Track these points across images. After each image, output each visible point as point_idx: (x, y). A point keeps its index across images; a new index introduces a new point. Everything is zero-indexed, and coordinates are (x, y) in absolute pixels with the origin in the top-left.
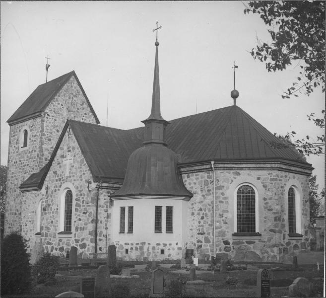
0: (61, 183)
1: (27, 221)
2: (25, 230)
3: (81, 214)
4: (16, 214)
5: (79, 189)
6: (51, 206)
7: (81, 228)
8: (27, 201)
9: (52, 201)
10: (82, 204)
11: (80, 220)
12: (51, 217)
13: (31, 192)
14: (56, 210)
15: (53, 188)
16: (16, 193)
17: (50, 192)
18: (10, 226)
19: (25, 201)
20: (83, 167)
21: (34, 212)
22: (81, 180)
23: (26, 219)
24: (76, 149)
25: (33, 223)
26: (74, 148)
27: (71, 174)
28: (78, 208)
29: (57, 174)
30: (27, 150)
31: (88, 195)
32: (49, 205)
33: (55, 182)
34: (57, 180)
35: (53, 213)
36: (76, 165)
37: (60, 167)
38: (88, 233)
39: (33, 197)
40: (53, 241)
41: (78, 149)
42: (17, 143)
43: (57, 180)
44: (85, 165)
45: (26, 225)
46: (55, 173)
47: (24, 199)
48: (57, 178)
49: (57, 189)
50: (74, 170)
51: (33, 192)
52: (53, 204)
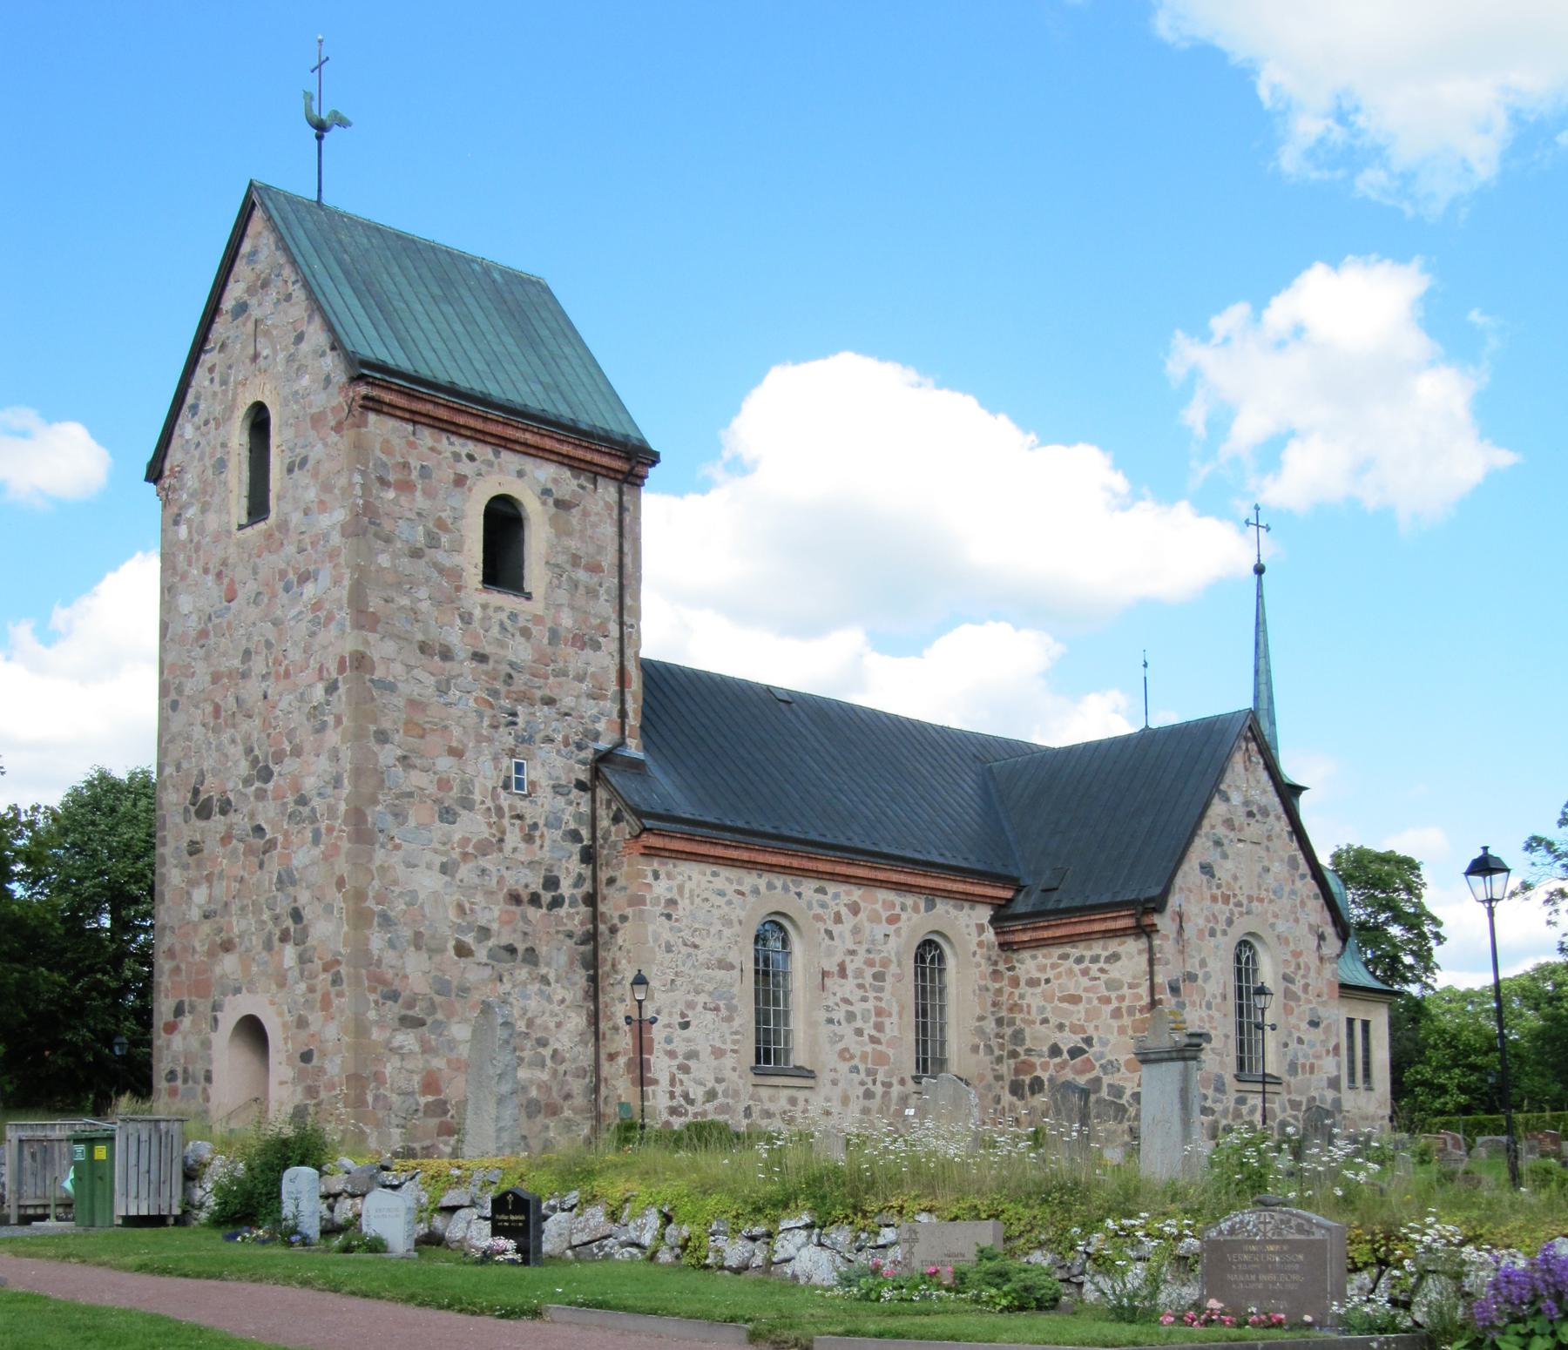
0: (1232, 913)
1: (691, 1005)
2: (680, 1047)
3: (1304, 1026)
4: (462, 951)
5: (1292, 947)
6: (1200, 981)
7: (1304, 1066)
8: (684, 903)
9: (1203, 963)
10: (1303, 996)
11: (1300, 1041)
12: (1201, 1019)
13: (709, 869)
14: (1219, 1000)
15: (1201, 922)
16: (457, 832)
17: (1190, 931)
18: (417, 1012)
19: (672, 902)
20: (1299, 884)
21: (732, 967)
22: (1297, 920)
23: (680, 996)
24: (1272, 817)
25: (729, 1019)
26: (1265, 812)
27: (1263, 894)
28: (1293, 1004)
29: (1213, 876)
30: (538, 620)
31: (1319, 972)
32: (1191, 977)
33: (1208, 902)
34: (1214, 899)
35: (1209, 1006)
36: (1278, 868)
37: (1225, 856)
38: (1325, 1083)
39: (721, 894)
40: (1215, 1101)
41: (1278, 818)
42: (433, 541)
43: (1214, 899)
44: (1303, 877)
45: (685, 1026)
46: (1207, 869)
47: (661, 888)
48: (1215, 891)
49: (1219, 928)
50: (1270, 880)
51: (725, 872)
52: (1207, 977)
